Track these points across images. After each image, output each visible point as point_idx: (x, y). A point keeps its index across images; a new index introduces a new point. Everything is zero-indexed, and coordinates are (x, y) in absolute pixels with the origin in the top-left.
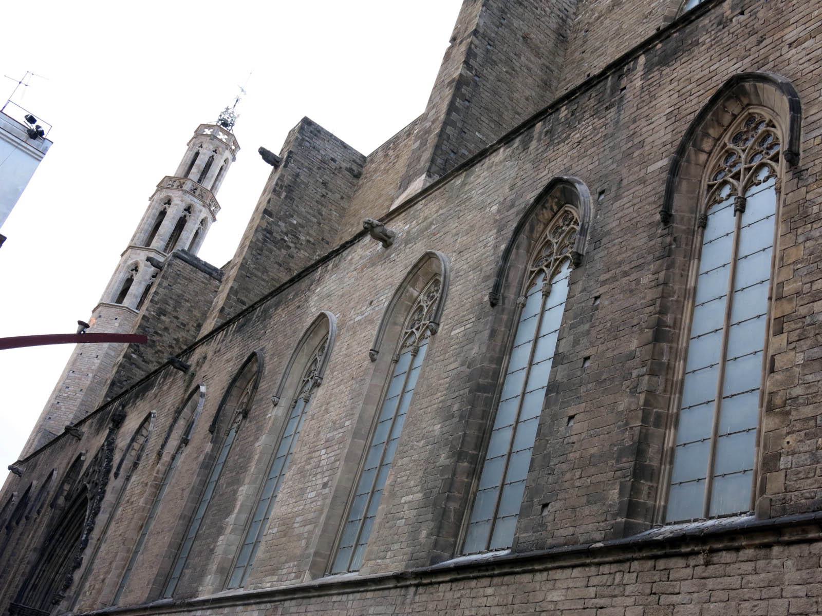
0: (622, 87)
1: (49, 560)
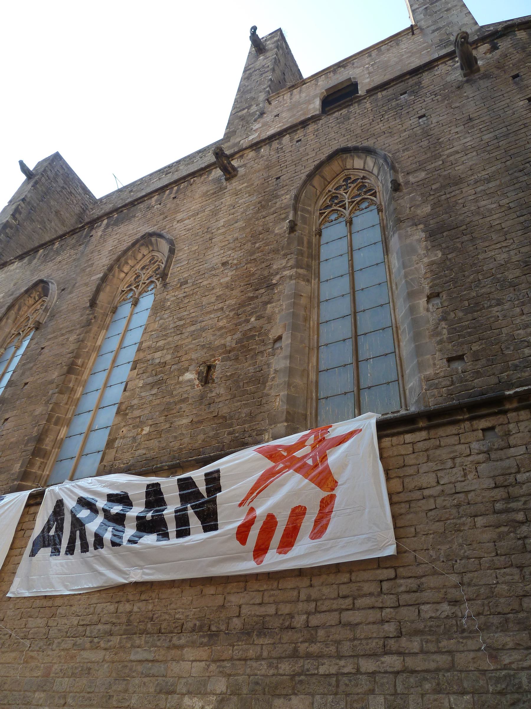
0: (91, 235)
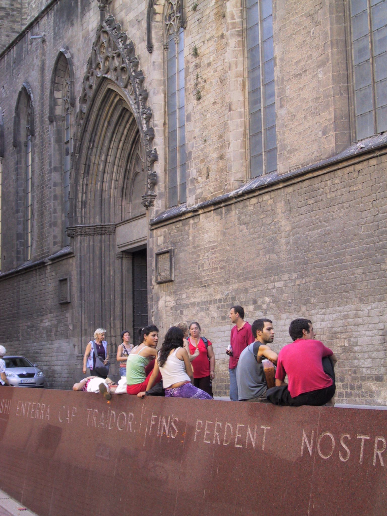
1: (87, 171)
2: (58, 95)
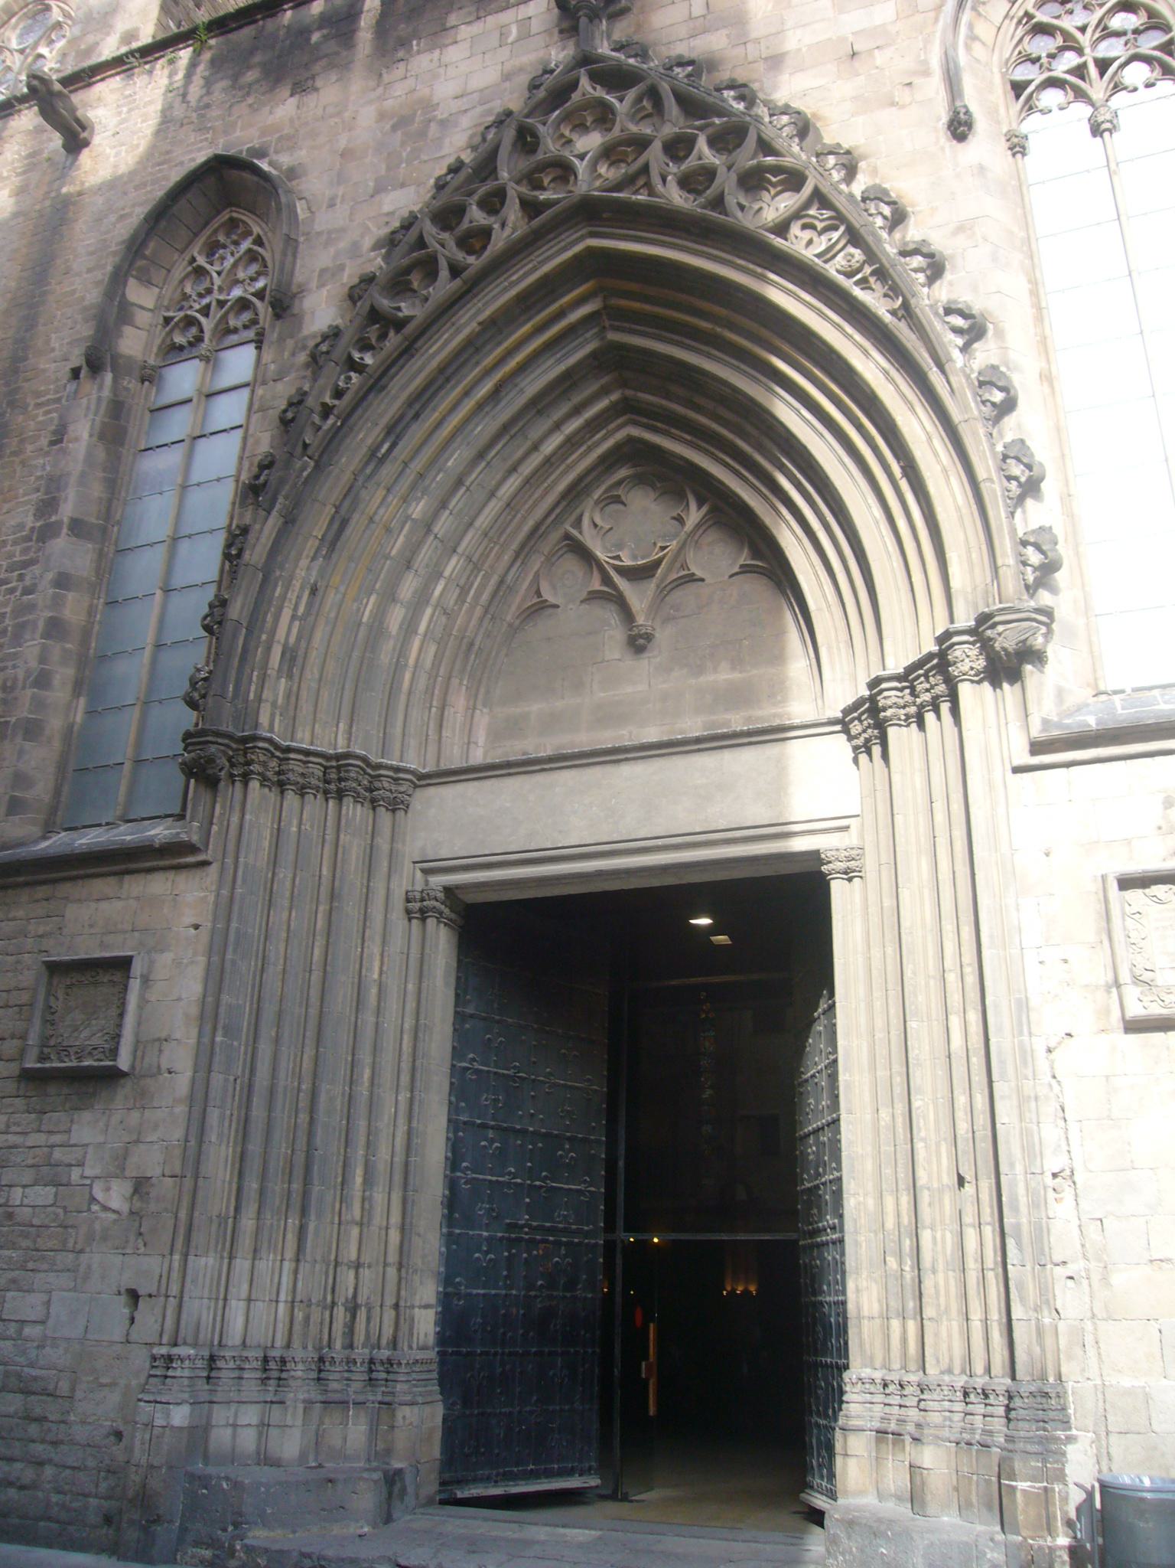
2: (139, 295)
